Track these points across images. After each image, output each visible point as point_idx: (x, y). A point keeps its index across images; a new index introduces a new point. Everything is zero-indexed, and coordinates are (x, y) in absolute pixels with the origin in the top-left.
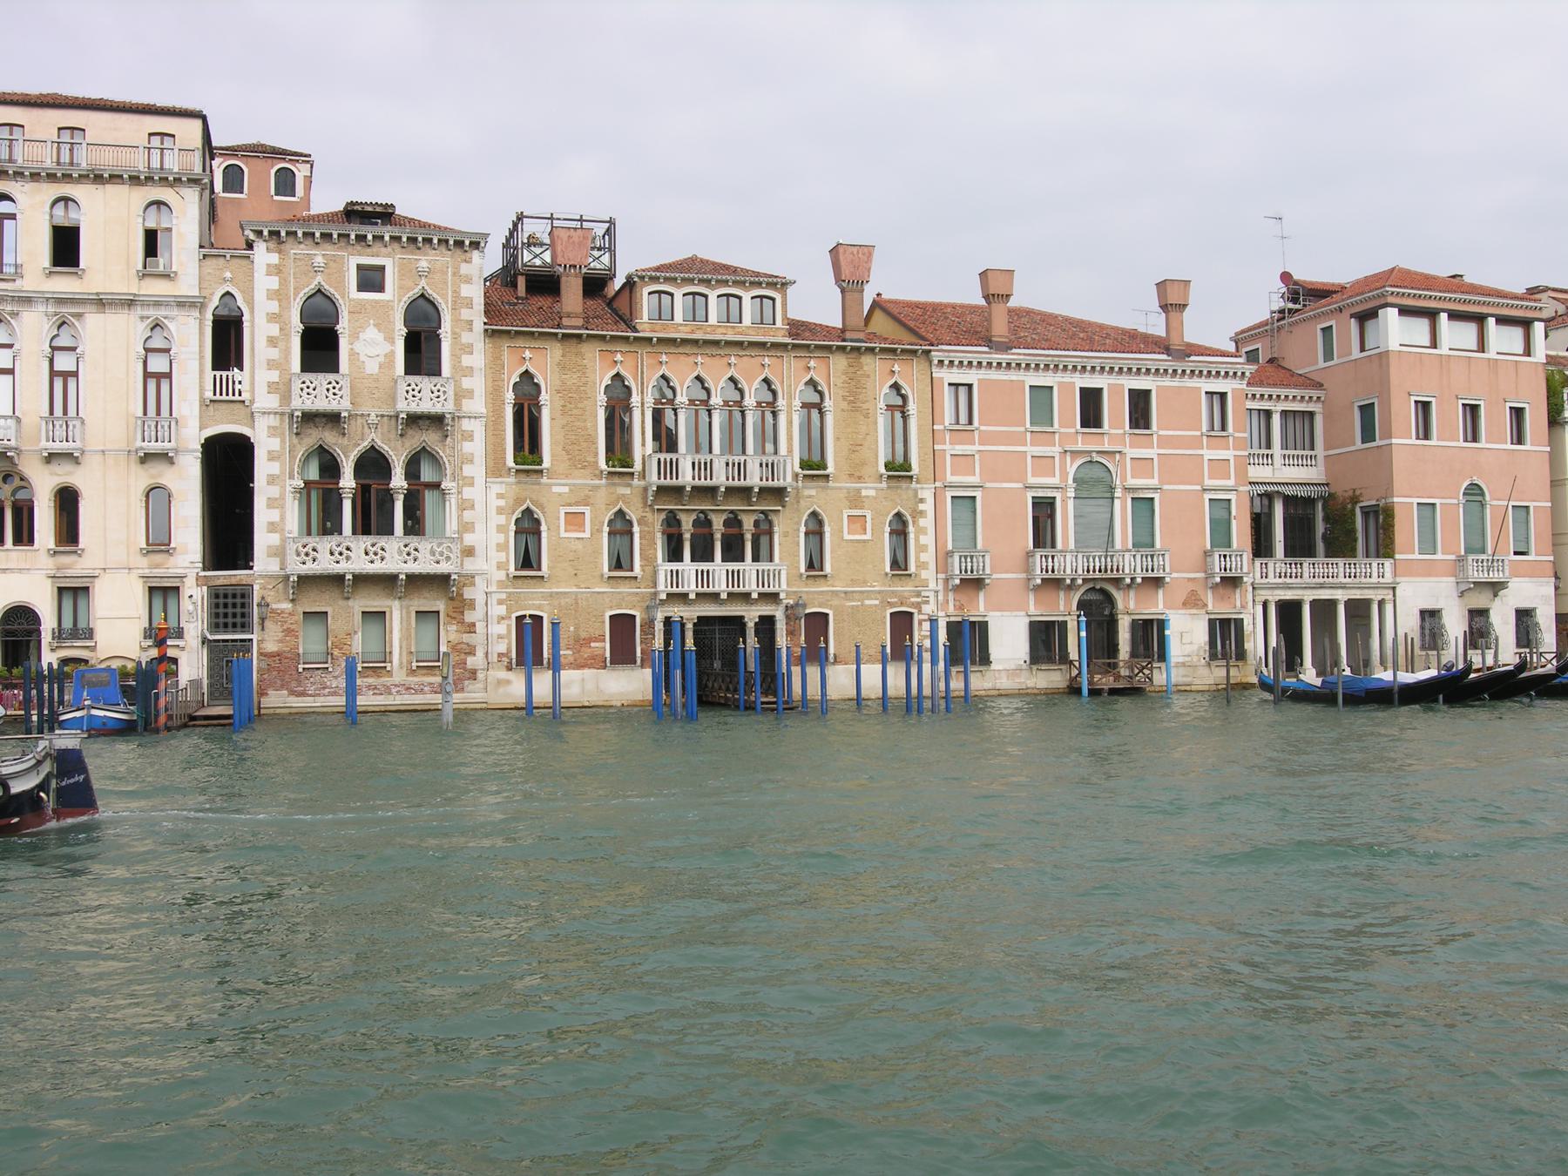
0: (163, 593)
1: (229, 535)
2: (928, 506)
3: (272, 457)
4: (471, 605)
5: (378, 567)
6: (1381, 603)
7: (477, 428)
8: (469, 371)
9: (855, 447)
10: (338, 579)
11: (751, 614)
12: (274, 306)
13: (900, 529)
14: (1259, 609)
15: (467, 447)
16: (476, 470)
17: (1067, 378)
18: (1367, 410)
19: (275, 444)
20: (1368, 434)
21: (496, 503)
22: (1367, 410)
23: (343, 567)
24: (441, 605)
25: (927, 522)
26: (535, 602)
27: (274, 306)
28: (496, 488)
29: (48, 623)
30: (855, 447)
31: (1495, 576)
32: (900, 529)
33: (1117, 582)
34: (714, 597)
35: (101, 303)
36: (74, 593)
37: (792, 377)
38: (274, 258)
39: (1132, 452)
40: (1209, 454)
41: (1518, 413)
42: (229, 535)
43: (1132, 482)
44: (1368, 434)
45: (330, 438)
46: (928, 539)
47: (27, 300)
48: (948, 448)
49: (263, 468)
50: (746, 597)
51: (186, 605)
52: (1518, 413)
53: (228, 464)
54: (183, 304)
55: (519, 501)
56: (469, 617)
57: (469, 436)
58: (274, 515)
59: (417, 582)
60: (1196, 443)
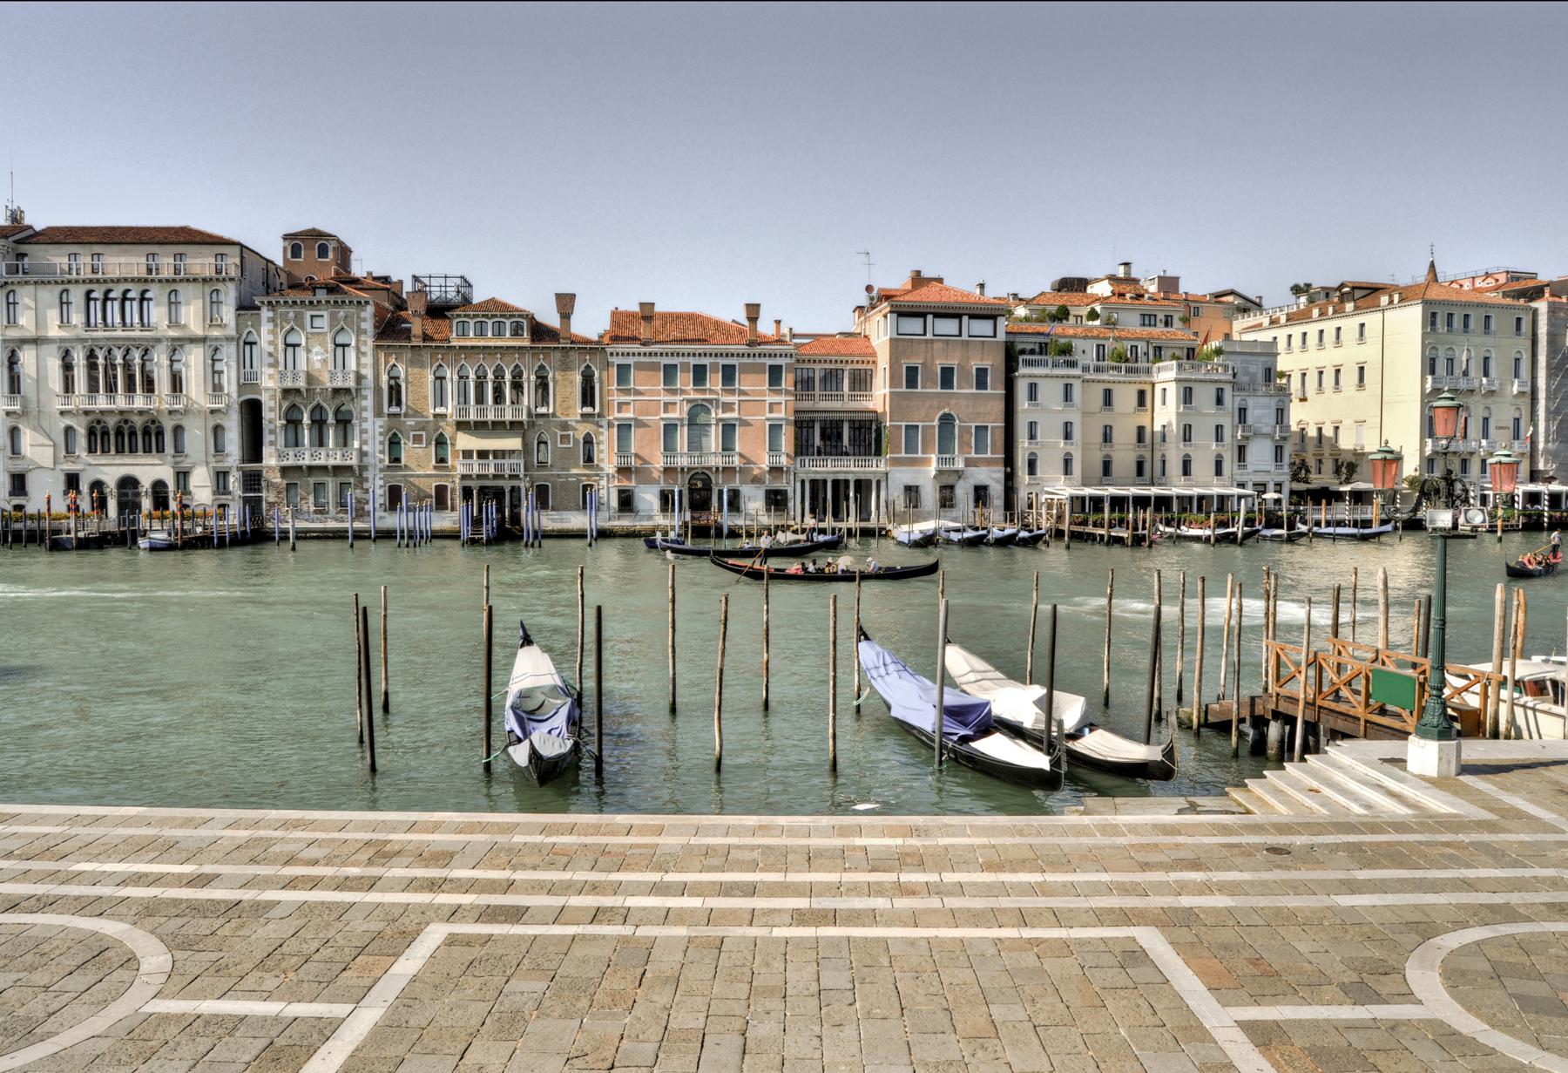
0: (221, 476)
1: (253, 448)
3: (271, 410)
4: (367, 480)
5: (317, 462)
6: (878, 482)
7: (369, 394)
8: (365, 366)
10: (300, 468)
11: (507, 485)
12: (271, 338)
14: (798, 485)
15: (364, 403)
16: (369, 414)
17: (686, 360)
19: (272, 403)
21: (379, 430)
23: (301, 463)
24: (352, 480)
26: (397, 478)
27: (271, 338)
28: (380, 422)
29: (171, 487)
34: (486, 477)
35: (193, 340)
36: (182, 476)
38: (271, 314)
42: (253, 448)
43: (721, 415)
45: (298, 400)
47: (158, 340)
49: (267, 415)
50: (502, 477)
51: (232, 480)
53: (252, 411)
54: (228, 339)
55: (390, 429)
56: (366, 485)
57: (365, 398)
58: (272, 438)
59: (337, 470)
60: (762, 393)
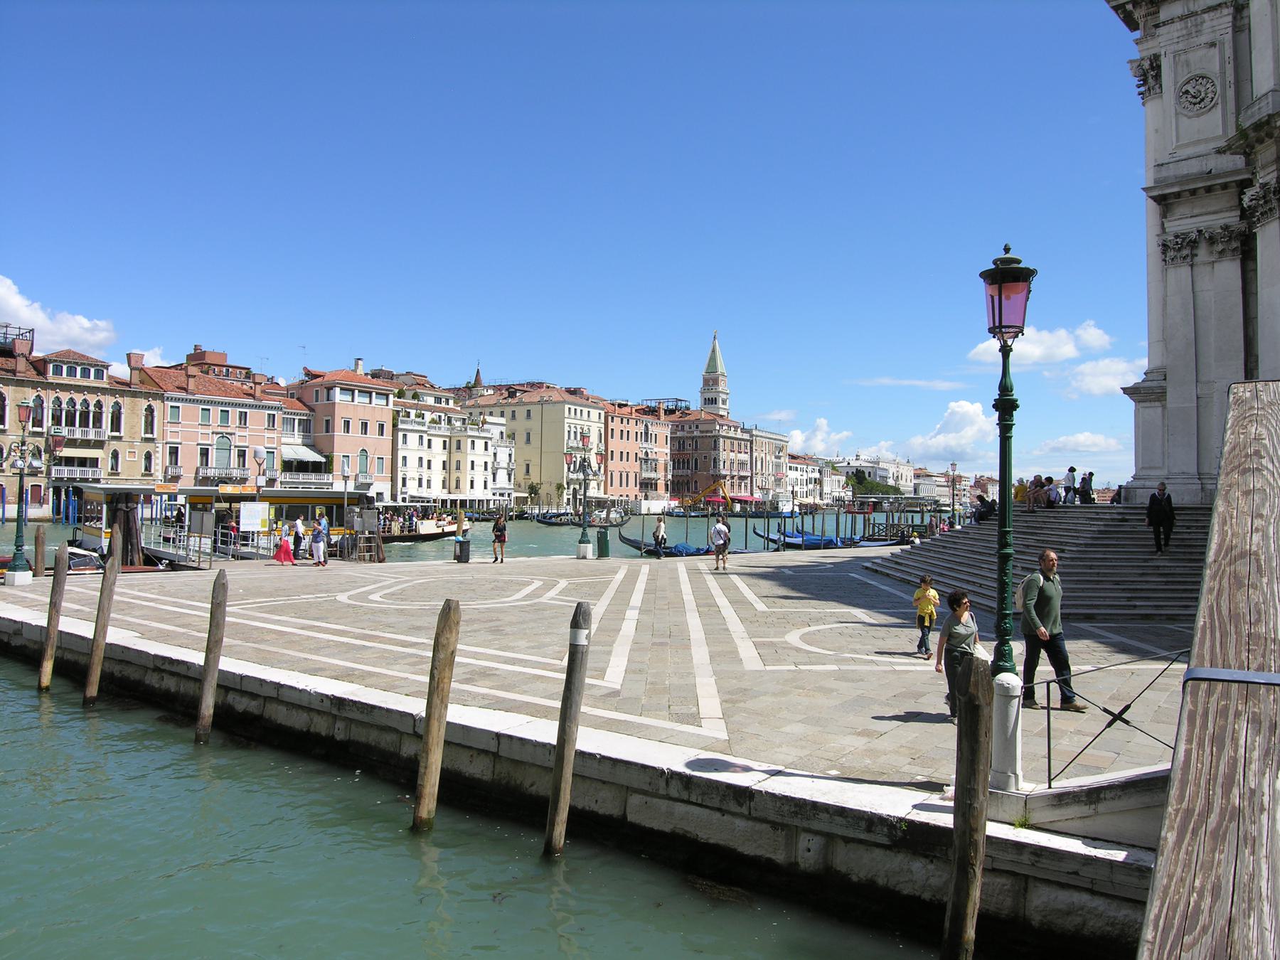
2: (160, 449)
9: (133, 427)
13: (148, 457)
18: (327, 421)
20: (327, 431)
22: (327, 421)
25: (159, 455)
30: (133, 427)
31: (368, 481)
32: (148, 457)
33: (230, 479)
37: (108, 402)
39: (238, 433)
40: (267, 435)
41: (381, 427)
44: (327, 431)
46: (159, 461)
48: (169, 428)
52: (381, 427)
